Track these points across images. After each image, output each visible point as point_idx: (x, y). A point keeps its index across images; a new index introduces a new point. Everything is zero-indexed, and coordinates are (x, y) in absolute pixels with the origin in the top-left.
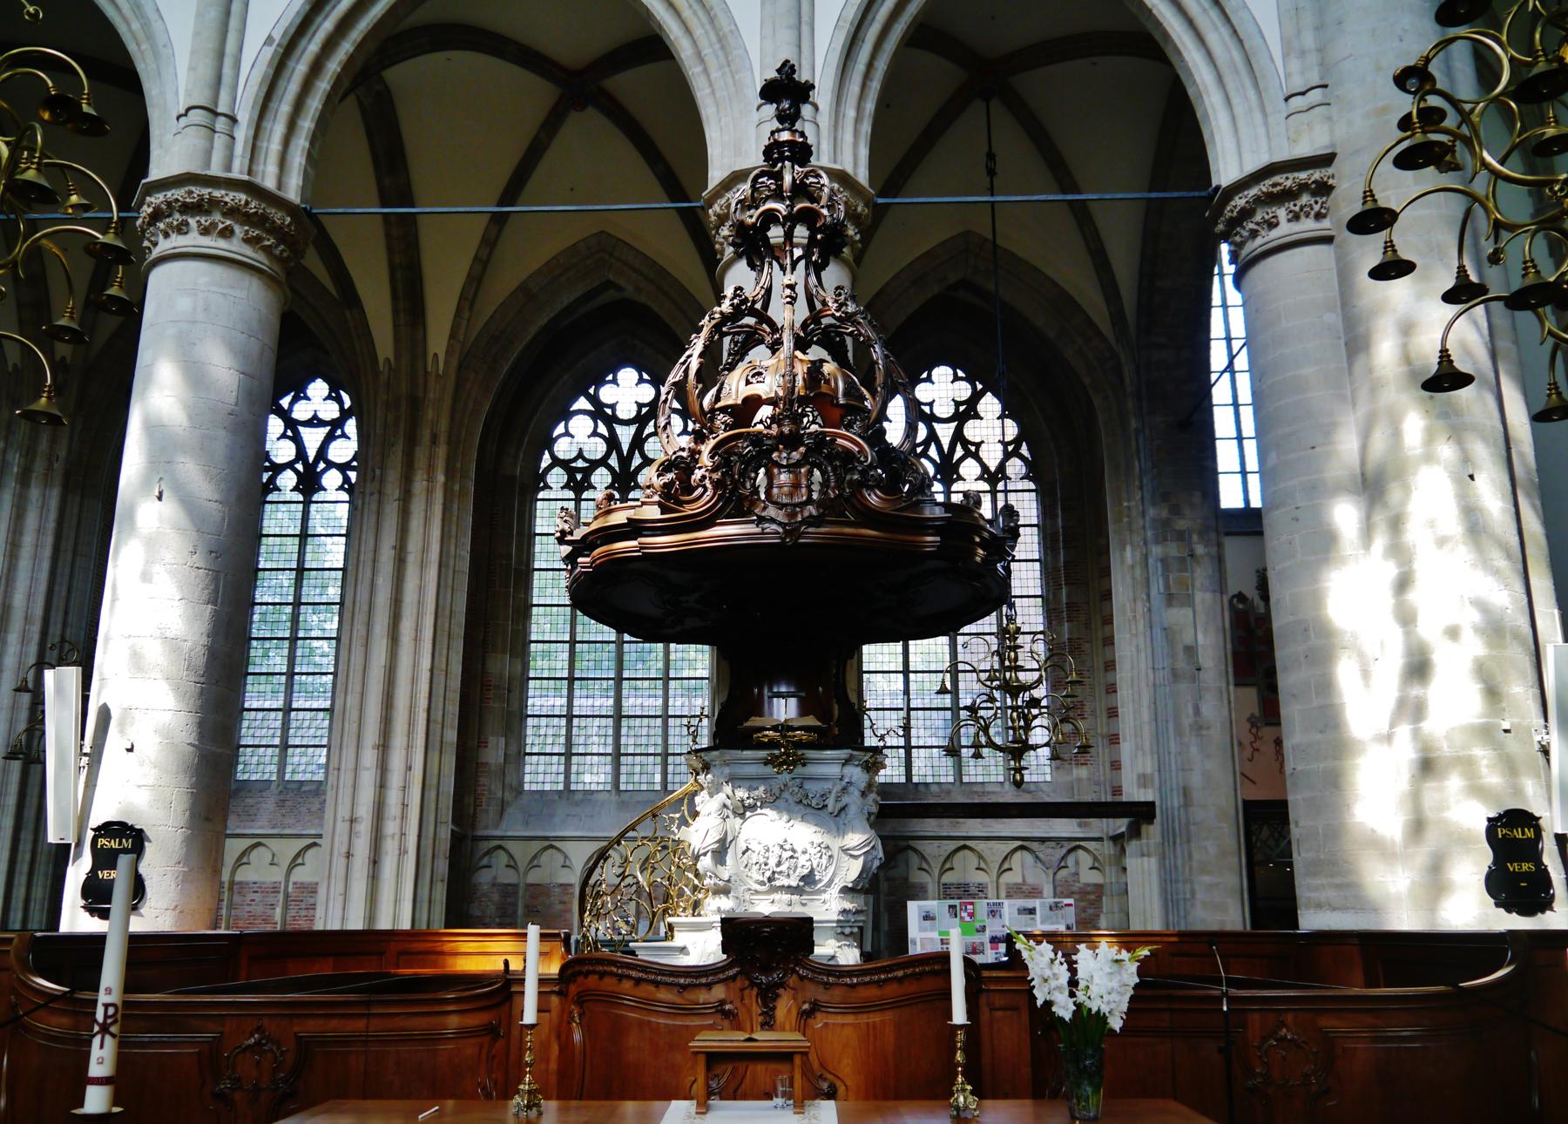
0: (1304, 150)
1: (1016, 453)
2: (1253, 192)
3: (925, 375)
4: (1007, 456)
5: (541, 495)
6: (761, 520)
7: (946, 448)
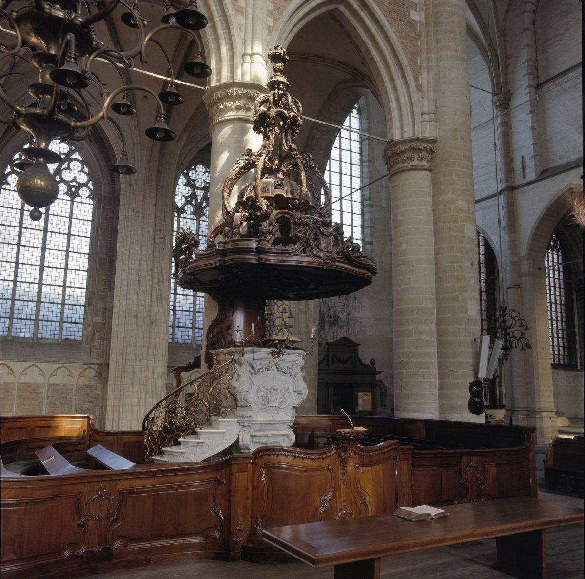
0: (427, 135)
1: (190, 202)
2: (407, 146)
3: (193, 167)
4: (187, 203)
5: (4, 187)
6: (315, 256)
7: (199, 201)
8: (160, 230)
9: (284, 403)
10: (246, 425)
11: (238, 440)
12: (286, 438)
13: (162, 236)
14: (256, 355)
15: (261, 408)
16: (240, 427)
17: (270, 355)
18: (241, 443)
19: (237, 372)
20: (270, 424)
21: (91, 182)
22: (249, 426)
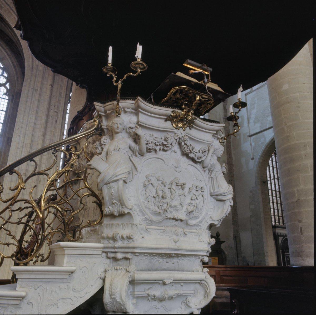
8: (55, 106)
9: (195, 214)
10: (119, 256)
11: (102, 290)
12: (198, 286)
13: (56, 110)
14: (143, 118)
15: (151, 222)
16: (108, 261)
17: (169, 123)
18: (107, 298)
19: (105, 150)
20: (169, 256)
21: (8, 84)
22: (126, 259)
